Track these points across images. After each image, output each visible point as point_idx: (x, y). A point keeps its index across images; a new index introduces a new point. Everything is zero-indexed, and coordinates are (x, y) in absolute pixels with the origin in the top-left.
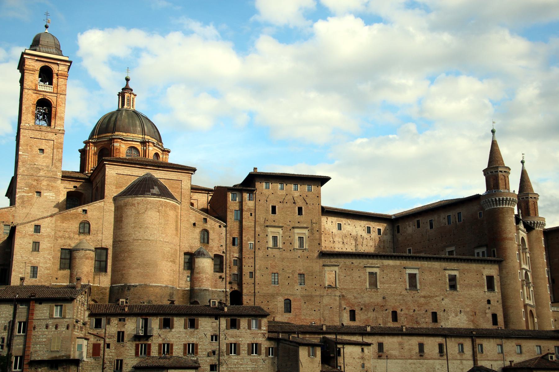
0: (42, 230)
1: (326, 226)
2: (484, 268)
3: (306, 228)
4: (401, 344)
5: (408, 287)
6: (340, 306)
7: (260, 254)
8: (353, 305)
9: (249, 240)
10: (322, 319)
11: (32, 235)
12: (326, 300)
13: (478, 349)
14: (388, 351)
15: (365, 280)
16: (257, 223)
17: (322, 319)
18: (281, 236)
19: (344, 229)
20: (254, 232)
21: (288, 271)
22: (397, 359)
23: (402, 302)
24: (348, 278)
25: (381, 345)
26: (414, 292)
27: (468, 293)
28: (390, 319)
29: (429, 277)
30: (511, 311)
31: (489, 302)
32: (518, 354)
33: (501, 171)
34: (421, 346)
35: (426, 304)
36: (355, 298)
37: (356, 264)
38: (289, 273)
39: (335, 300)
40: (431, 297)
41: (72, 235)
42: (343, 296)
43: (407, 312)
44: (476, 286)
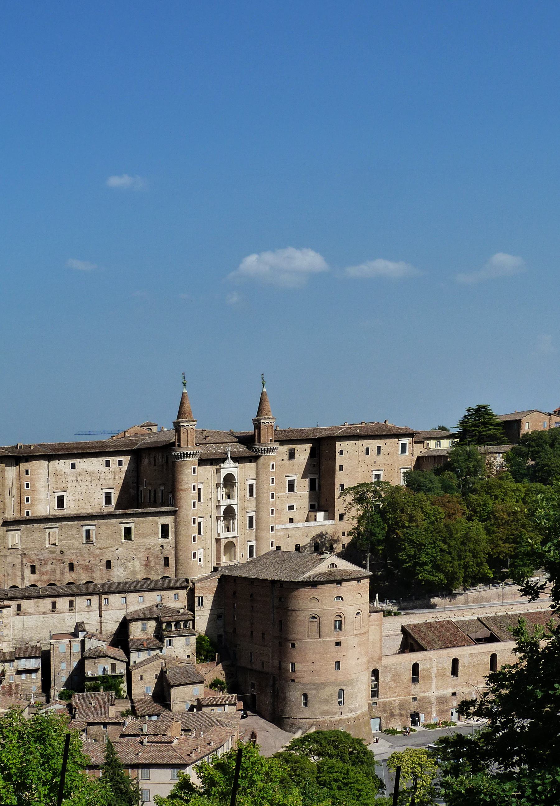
1: (58, 468)
4: (35, 603)
5: (84, 542)
6: (22, 563)
8: (34, 561)
10: (6, 574)
12: (9, 559)
13: (104, 602)
14: (25, 609)
17: (6, 574)
19: (78, 467)
22: (32, 614)
23: (78, 554)
24: (29, 539)
25: (19, 607)
26: (90, 545)
28: (67, 569)
29: (105, 531)
30: (180, 554)
31: (162, 546)
32: (140, 603)
34: (54, 605)
35: (101, 554)
36: (36, 555)
39: (18, 558)
40: (107, 548)
42: (25, 554)
43: (83, 563)
44: (150, 535)
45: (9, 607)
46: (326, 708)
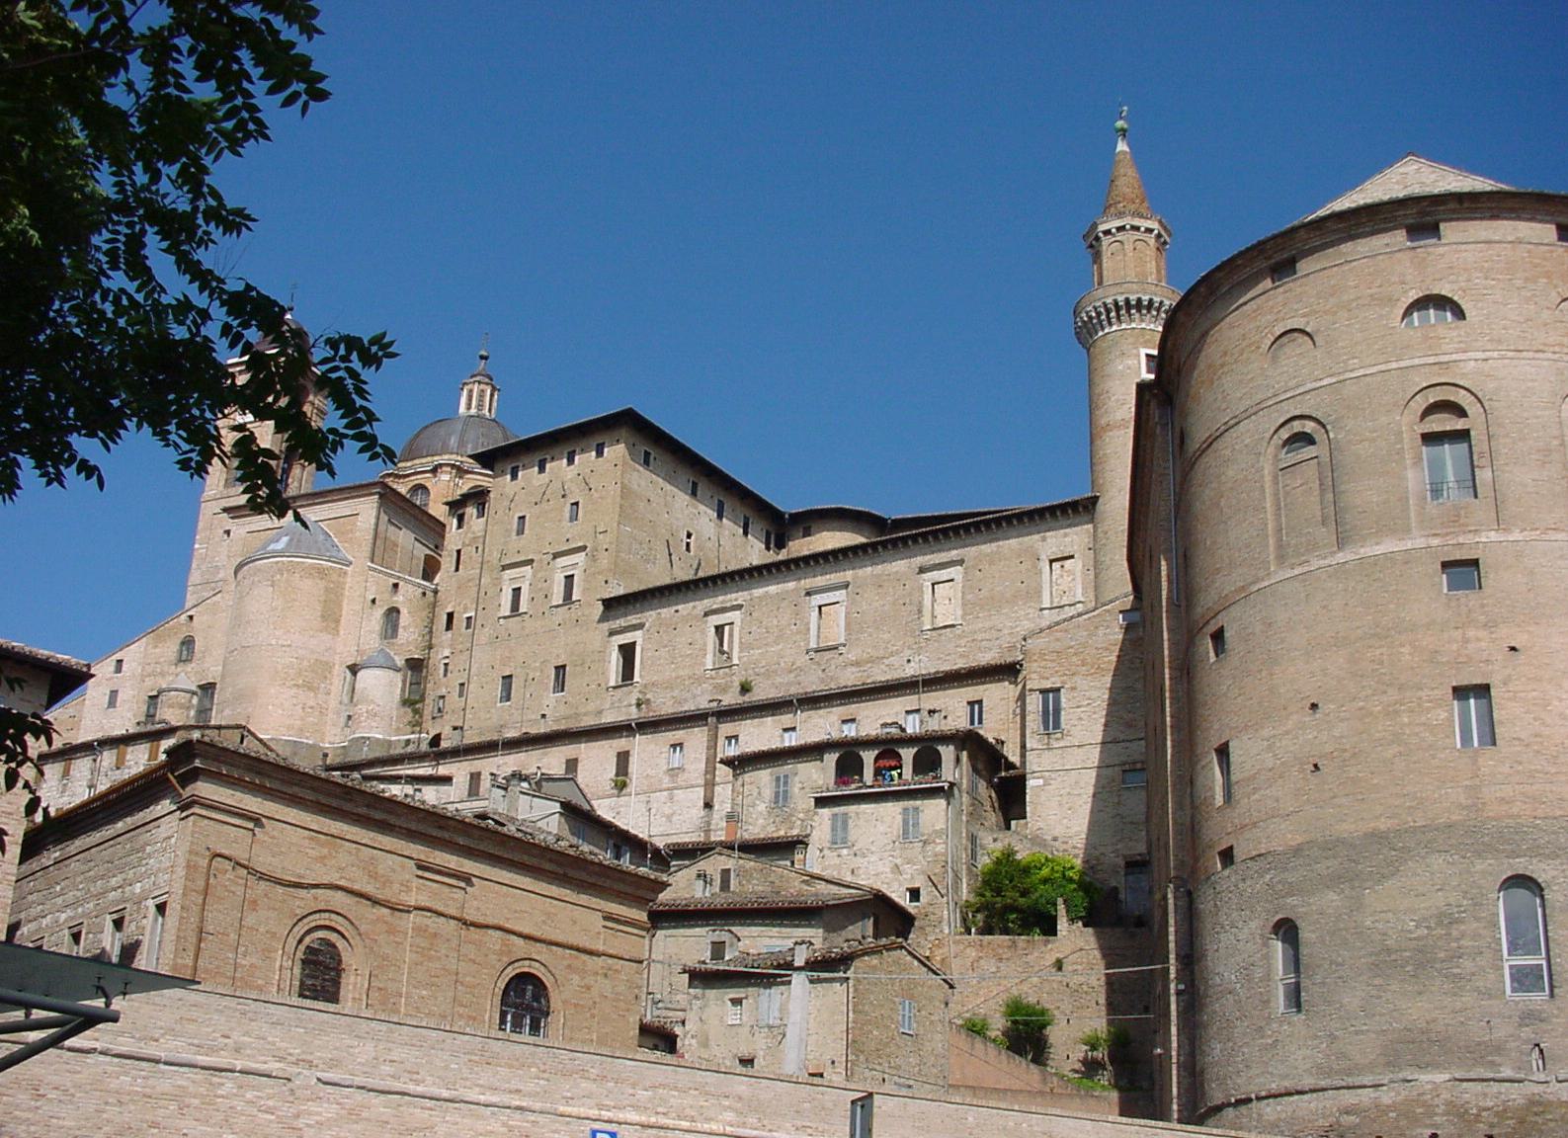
0: (125, 667)
2: (1044, 539)
3: (584, 548)
7: (483, 635)
9: (466, 610)
11: (112, 678)
15: (704, 650)
16: (485, 567)
18: (528, 583)
20: (476, 589)
21: (533, 665)
24: (663, 652)
27: (988, 624)
33: (1107, 232)
37: (685, 613)
38: (535, 669)
41: (166, 669)
45: (447, 780)
46: (1420, 1007)
